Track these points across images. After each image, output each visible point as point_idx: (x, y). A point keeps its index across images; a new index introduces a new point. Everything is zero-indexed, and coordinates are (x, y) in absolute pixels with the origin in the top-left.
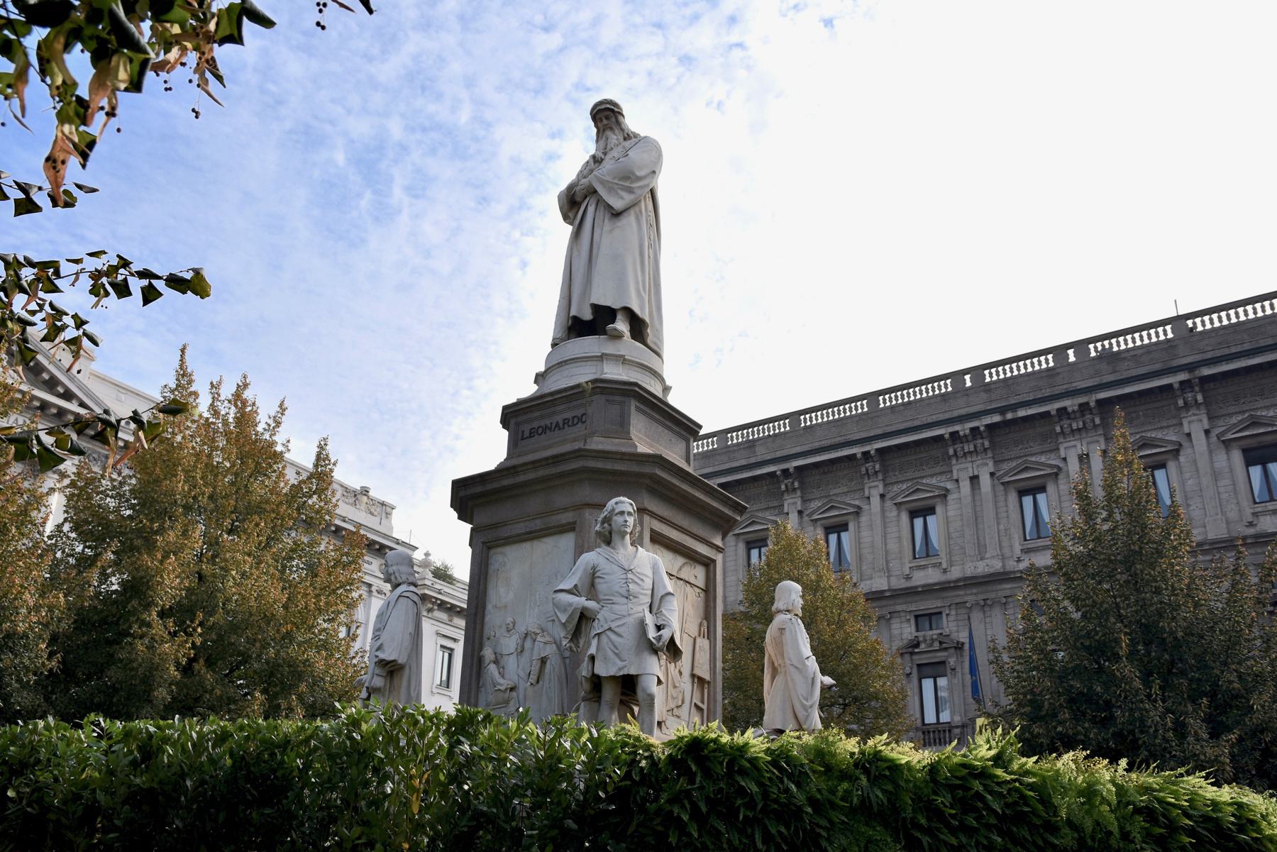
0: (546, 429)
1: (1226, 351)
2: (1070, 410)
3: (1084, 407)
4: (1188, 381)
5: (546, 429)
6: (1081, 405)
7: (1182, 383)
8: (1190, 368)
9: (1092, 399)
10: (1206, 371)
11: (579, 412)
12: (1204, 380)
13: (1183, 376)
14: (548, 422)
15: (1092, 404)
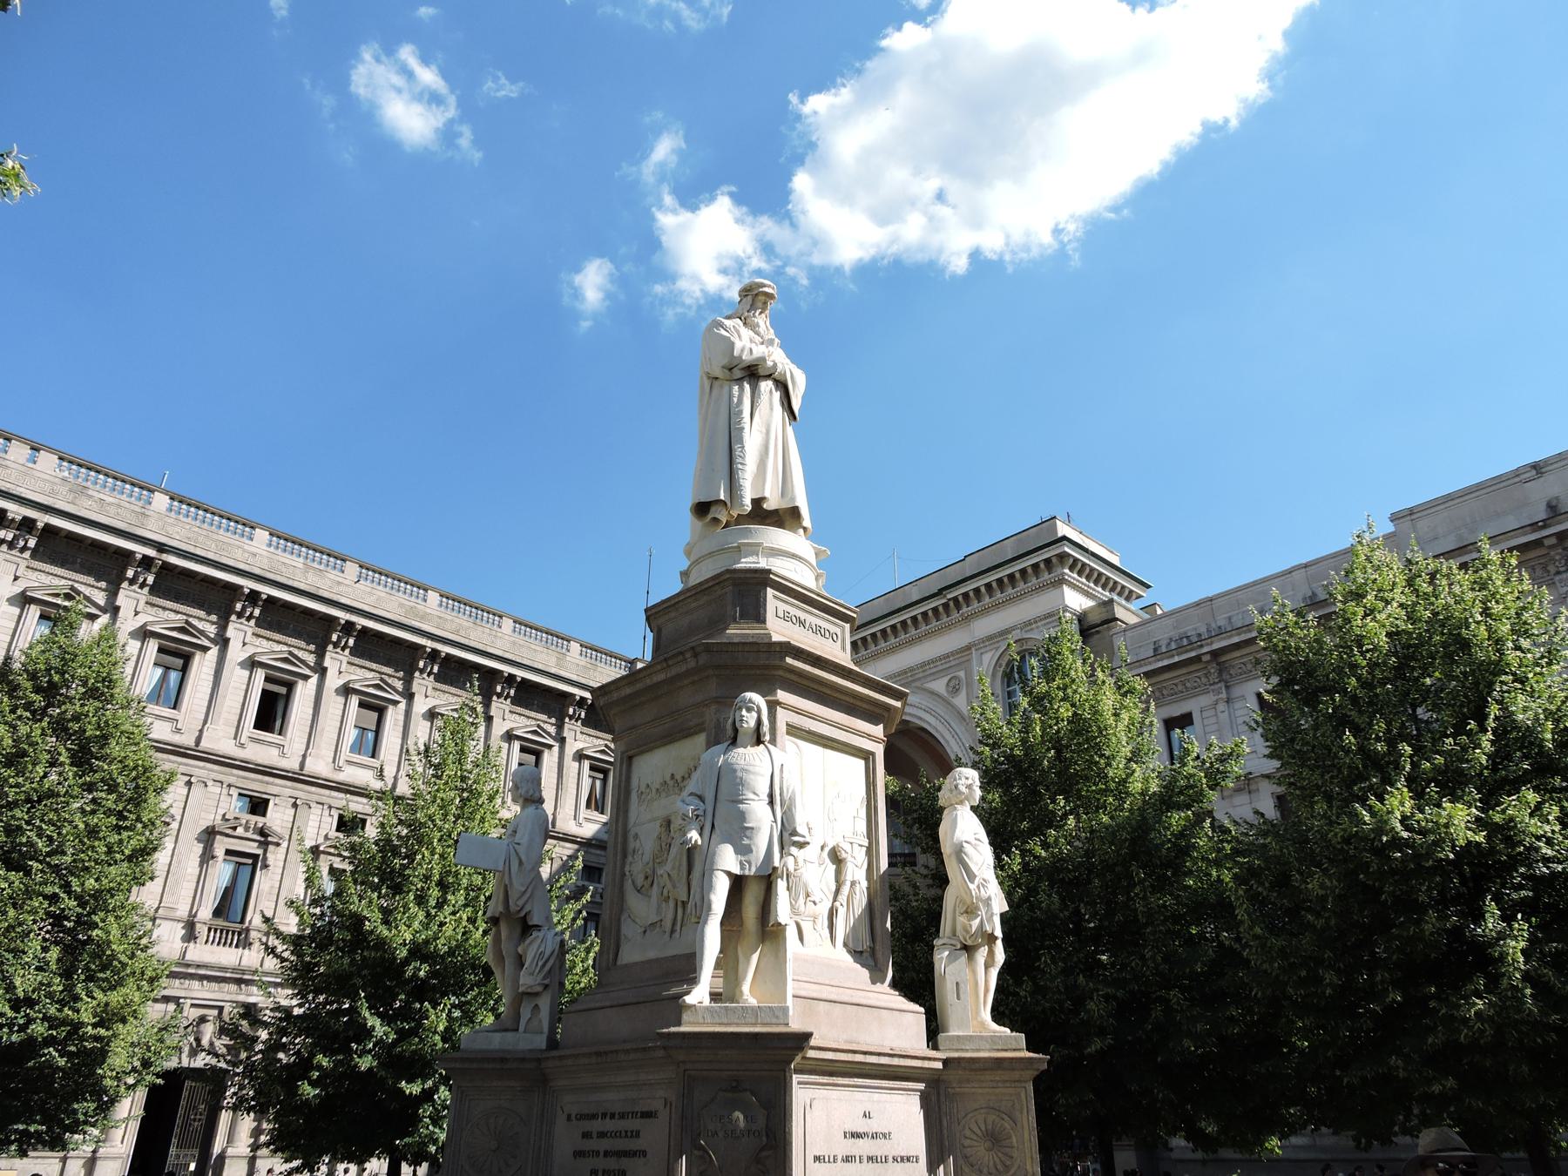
0: (802, 623)
1: (192, 550)
2: (10, 516)
3: (27, 525)
4: (152, 559)
5: (802, 623)
6: (25, 518)
7: (144, 556)
8: (161, 548)
9: (43, 519)
10: (173, 560)
11: (833, 629)
12: (166, 567)
13: (151, 553)
14: (803, 616)
15: (40, 525)
